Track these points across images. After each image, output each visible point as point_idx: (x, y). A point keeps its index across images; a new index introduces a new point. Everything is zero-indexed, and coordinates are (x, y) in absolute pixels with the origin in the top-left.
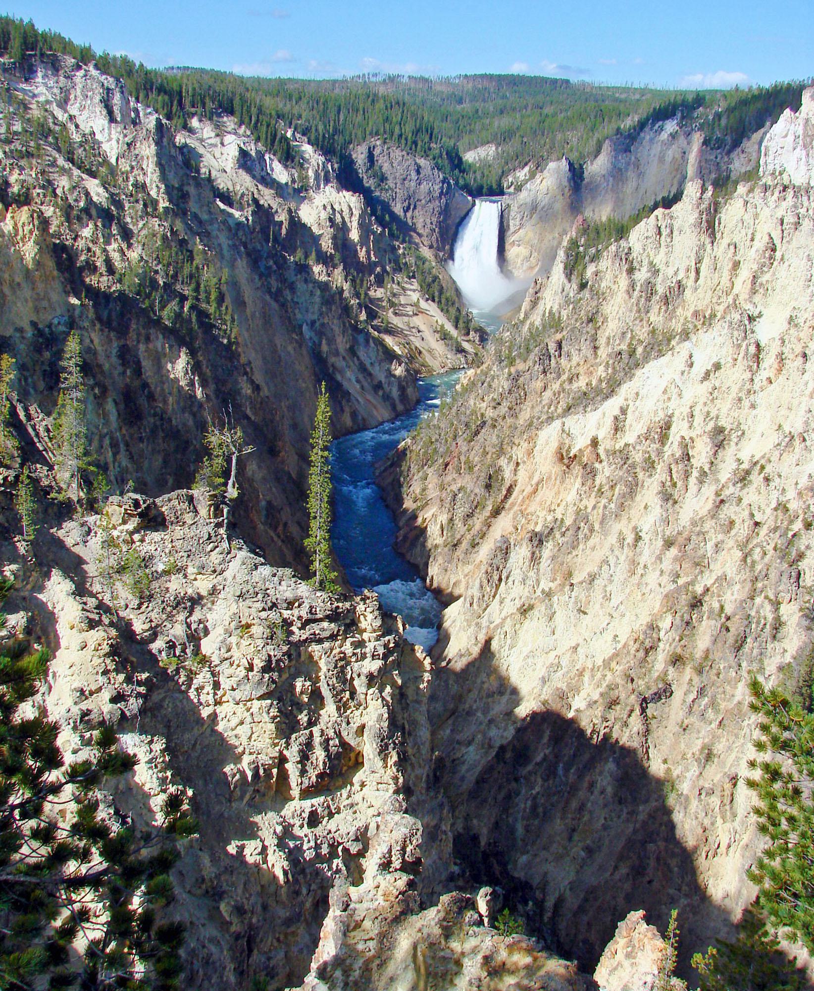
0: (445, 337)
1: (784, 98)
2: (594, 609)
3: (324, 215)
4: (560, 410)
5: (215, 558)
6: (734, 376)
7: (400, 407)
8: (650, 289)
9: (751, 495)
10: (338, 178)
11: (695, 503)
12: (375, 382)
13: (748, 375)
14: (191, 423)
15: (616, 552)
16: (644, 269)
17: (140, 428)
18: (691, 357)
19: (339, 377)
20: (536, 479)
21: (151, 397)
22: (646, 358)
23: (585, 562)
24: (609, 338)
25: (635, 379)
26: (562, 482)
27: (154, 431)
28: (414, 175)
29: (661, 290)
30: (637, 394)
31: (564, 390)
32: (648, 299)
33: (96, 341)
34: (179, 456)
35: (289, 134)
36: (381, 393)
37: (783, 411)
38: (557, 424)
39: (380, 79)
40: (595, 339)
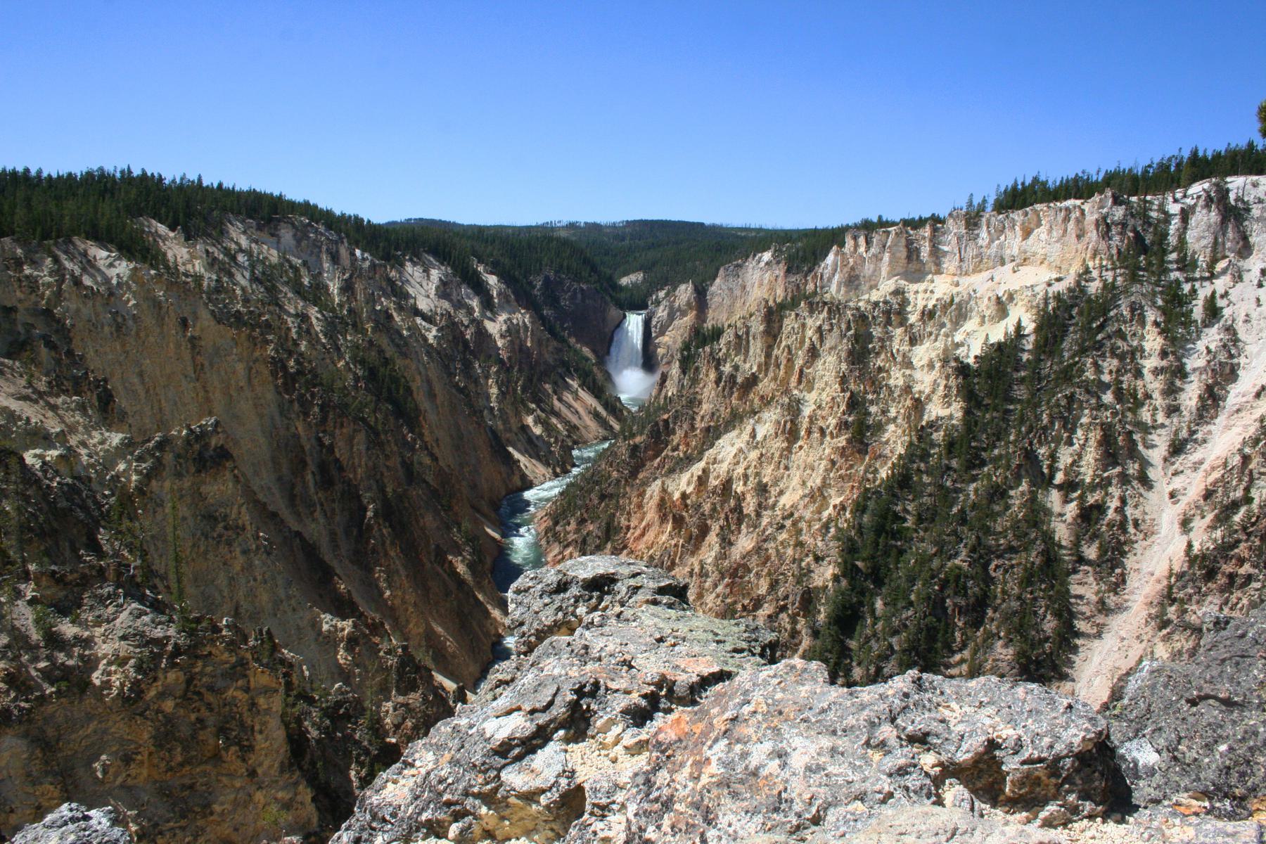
0: (596, 415)
1: (834, 237)
3: (504, 328)
5: (111, 609)
6: (779, 444)
8: (732, 377)
9: (783, 536)
10: (517, 301)
11: (745, 542)
13: (785, 445)
16: (728, 365)
18: (754, 430)
20: (644, 523)
22: (726, 431)
24: (703, 417)
28: (579, 296)
29: (739, 380)
32: (731, 388)
33: (300, 429)
35: (481, 268)
37: (808, 471)
38: (658, 482)
39: (564, 223)
40: (693, 419)
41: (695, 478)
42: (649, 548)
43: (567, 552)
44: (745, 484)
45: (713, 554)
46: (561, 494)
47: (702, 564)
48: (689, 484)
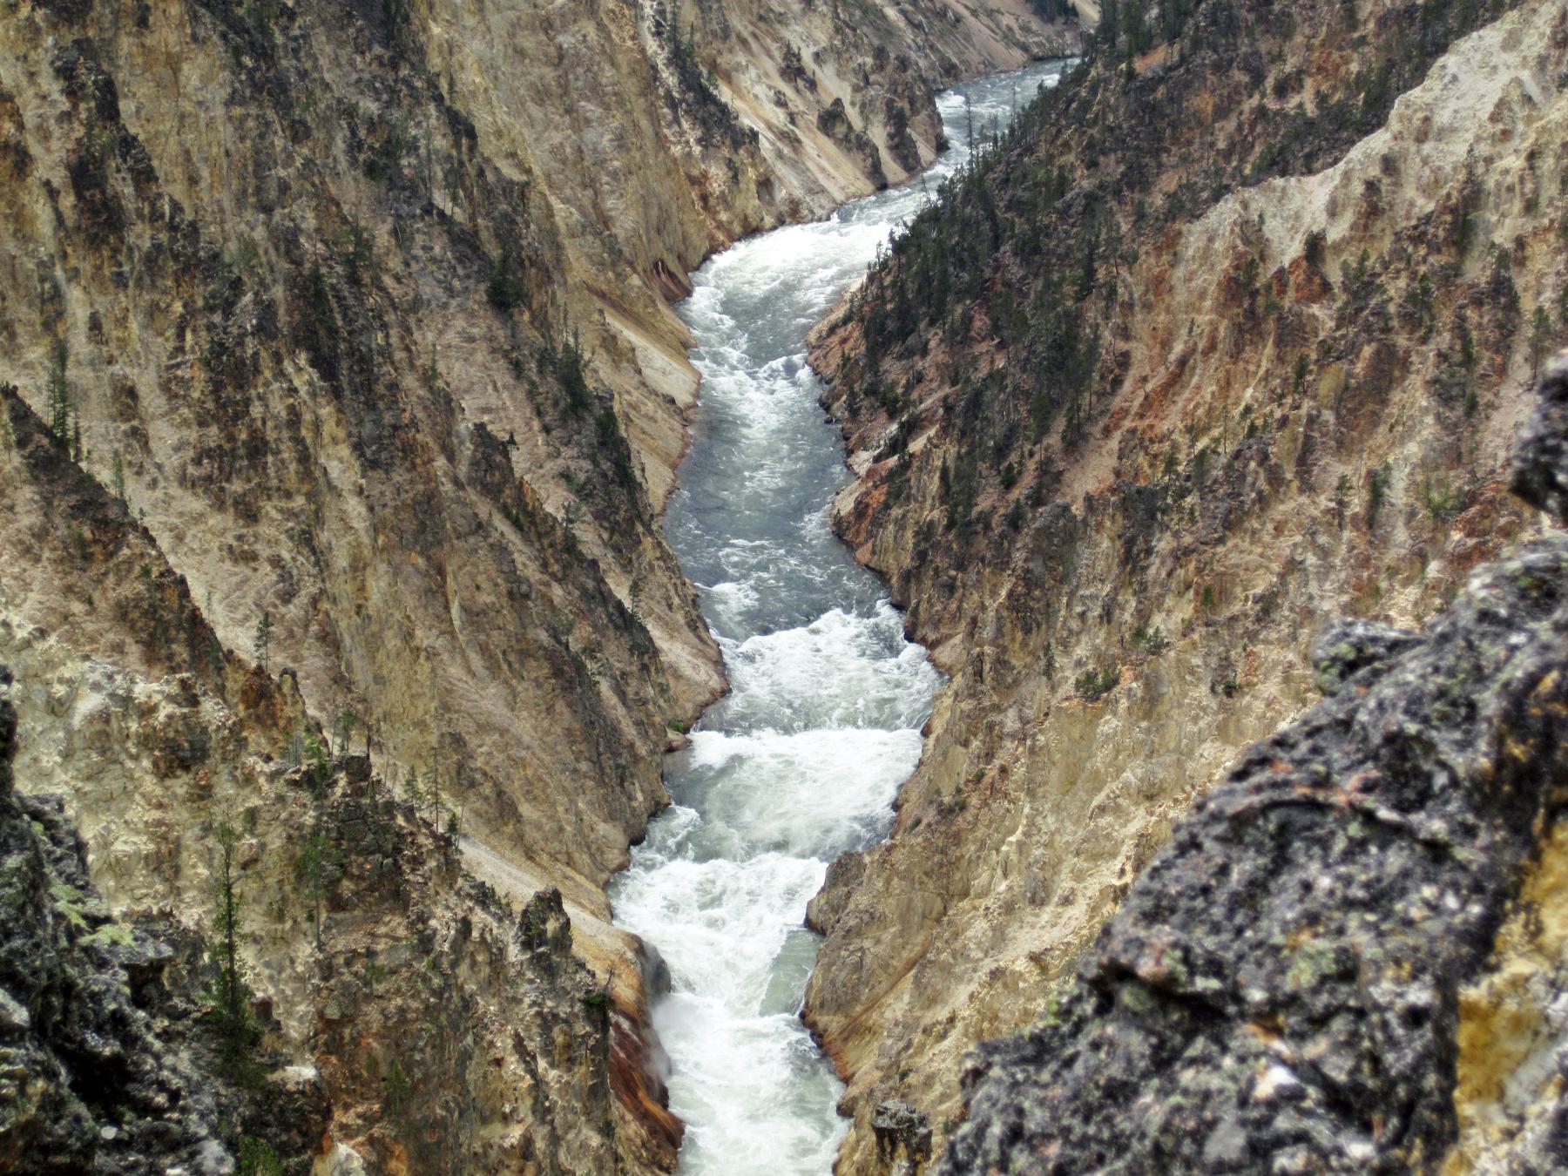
2: (1271, 687)
4: (1247, 171)
7: (892, 168)
12: (828, 102)
14: (259, 234)
15: (1322, 539)
17: (116, 251)
19: (725, 94)
20: (1178, 348)
21: (144, 177)
23: (1252, 560)
25: (1427, 83)
26: (1236, 354)
27: (151, 260)
30: (1427, 120)
31: (1261, 112)
34: (217, 318)
36: (840, 130)
41: (1358, 188)
42: (1194, 432)
43: (916, 446)
44: (1530, 207)
45: (1413, 449)
46: (900, 246)
47: (1377, 486)
48: (1333, 211)
